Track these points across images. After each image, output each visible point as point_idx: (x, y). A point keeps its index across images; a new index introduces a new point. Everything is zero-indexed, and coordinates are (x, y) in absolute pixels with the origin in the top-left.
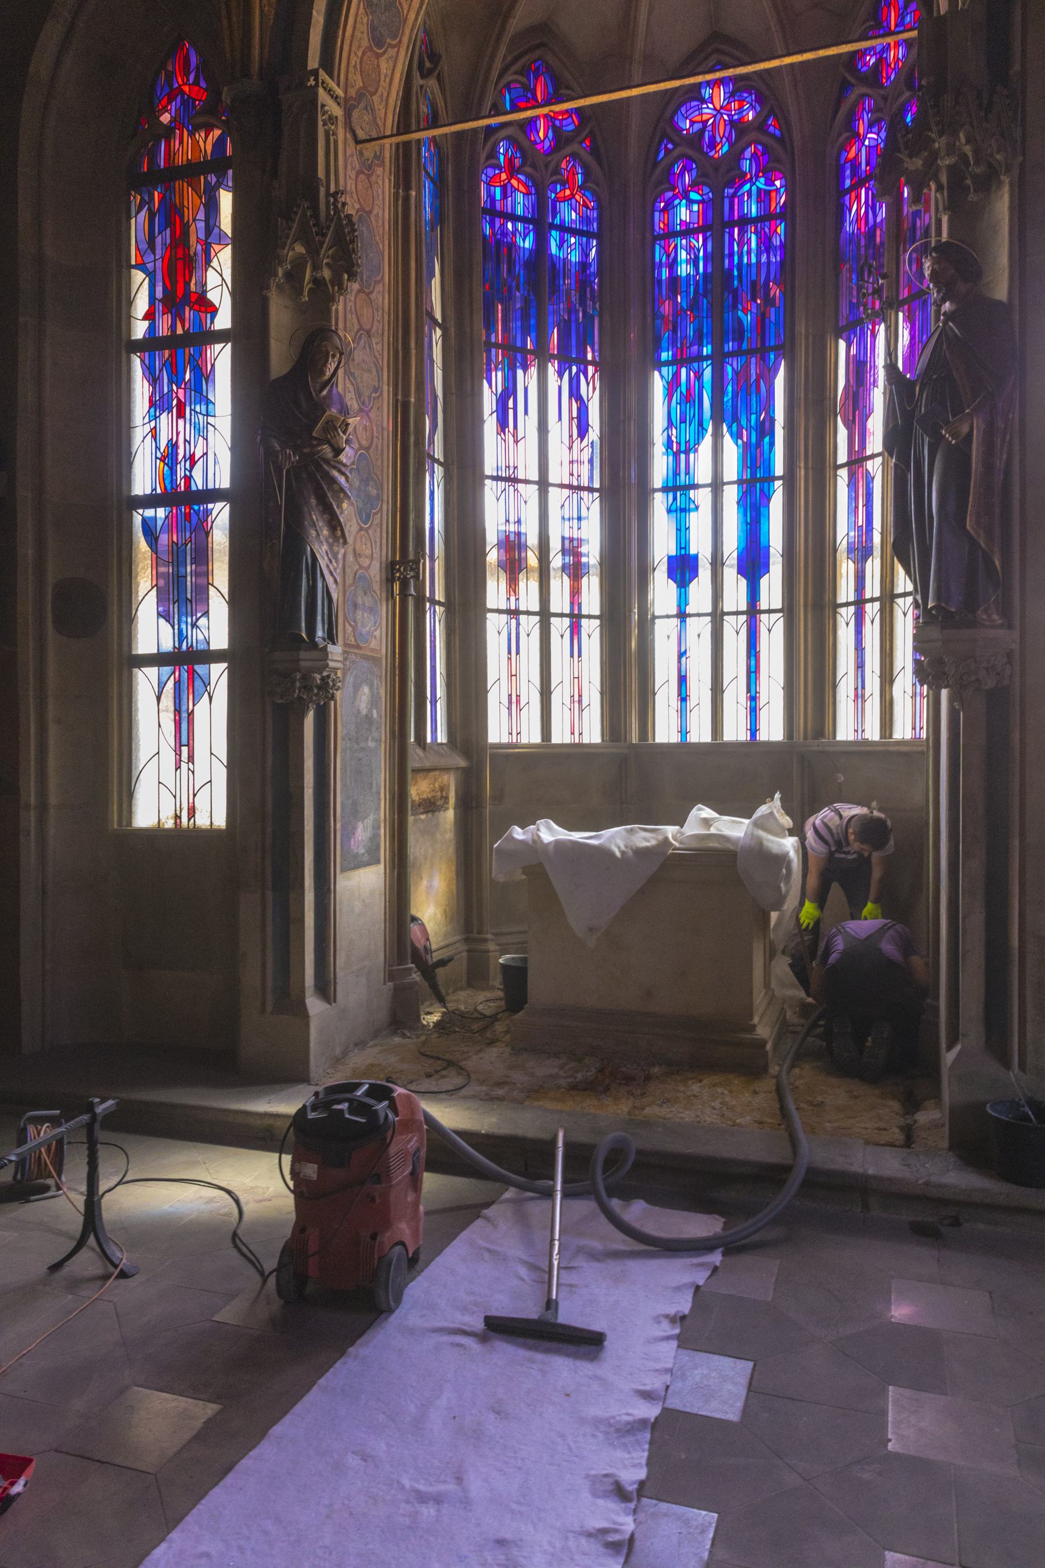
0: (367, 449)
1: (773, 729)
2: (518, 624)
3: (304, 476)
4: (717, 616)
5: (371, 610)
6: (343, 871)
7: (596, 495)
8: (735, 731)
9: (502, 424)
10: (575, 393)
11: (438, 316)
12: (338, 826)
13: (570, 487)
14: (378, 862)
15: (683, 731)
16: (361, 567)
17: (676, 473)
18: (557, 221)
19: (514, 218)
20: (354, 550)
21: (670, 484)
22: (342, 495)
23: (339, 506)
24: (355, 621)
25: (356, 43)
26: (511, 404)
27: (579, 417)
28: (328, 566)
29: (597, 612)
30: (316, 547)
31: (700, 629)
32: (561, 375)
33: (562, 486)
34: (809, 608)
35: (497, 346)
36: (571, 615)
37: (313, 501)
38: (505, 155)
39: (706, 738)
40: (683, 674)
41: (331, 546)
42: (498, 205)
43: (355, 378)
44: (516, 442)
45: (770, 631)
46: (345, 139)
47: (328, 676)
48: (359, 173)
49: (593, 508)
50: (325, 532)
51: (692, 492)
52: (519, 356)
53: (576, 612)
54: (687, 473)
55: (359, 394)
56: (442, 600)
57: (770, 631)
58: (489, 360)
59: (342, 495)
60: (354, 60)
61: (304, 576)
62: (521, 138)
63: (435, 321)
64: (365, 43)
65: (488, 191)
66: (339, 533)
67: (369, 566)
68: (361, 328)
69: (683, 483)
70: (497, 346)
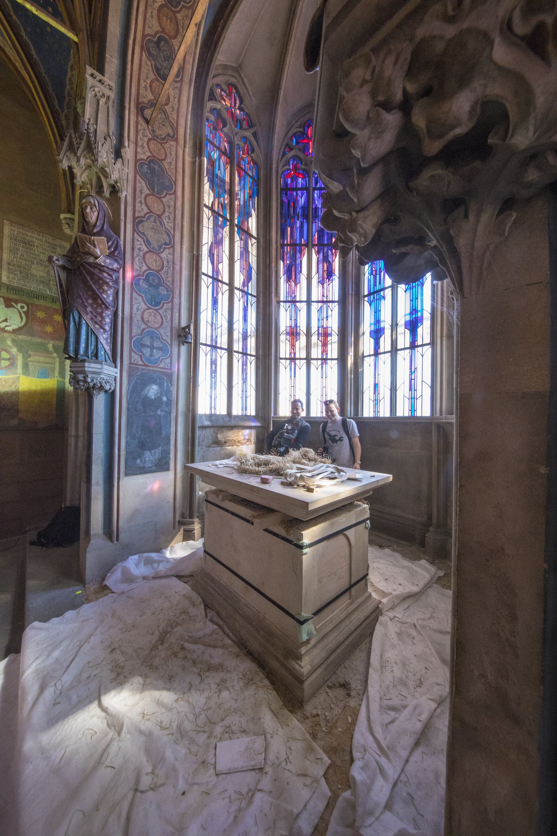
0: (158, 271)
1: (424, 410)
2: (295, 364)
3: (78, 273)
4: (394, 350)
5: (160, 349)
6: (126, 475)
7: (336, 304)
8: (403, 411)
9: (289, 279)
10: (326, 259)
11: (254, 232)
12: (123, 453)
13: (322, 302)
14: (168, 469)
15: (376, 410)
16: (149, 327)
17: (375, 285)
18: (318, 186)
19: (297, 189)
20: (142, 318)
21: (372, 291)
22: (101, 282)
23: (100, 287)
24: (142, 352)
25: (143, 76)
26: (293, 269)
27: (327, 270)
28: (92, 319)
29: (336, 357)
30: (80, 308)
31: (385, 359)
32: (318, 253)
33: (318, 302)
34: (444, 338)
35: (287, 245)
36: (322, 359)
37: (81, 285)
38: (293, 164)
39: (388, 415)
40: (377, 383)
41: (95, 309)
42: (289, 187)
43: (145, 235)
44: (296, 285)
45: (422, 356)
46: (137, 123)
47: (87, 376)
48: (149, 140)
49: (334, 311)
50: (90, 301)
51: (382, 292)
52: (298, 248)
53: (325, 357)
54: (380, 283)
55: (148, 243)
56: (254, 353)
57: (422, 356)
58: (283, 251)
59: (101, 282)
60: (143, 84)
61: (72, 324)
62: (301, 155)
63: (251, 236)
64: (152, 76)
65: (285, 180)
66: (100, 302)
67: (159, 327)
68: (151, 212)
69: (378, 289)
70: (287, 245)
